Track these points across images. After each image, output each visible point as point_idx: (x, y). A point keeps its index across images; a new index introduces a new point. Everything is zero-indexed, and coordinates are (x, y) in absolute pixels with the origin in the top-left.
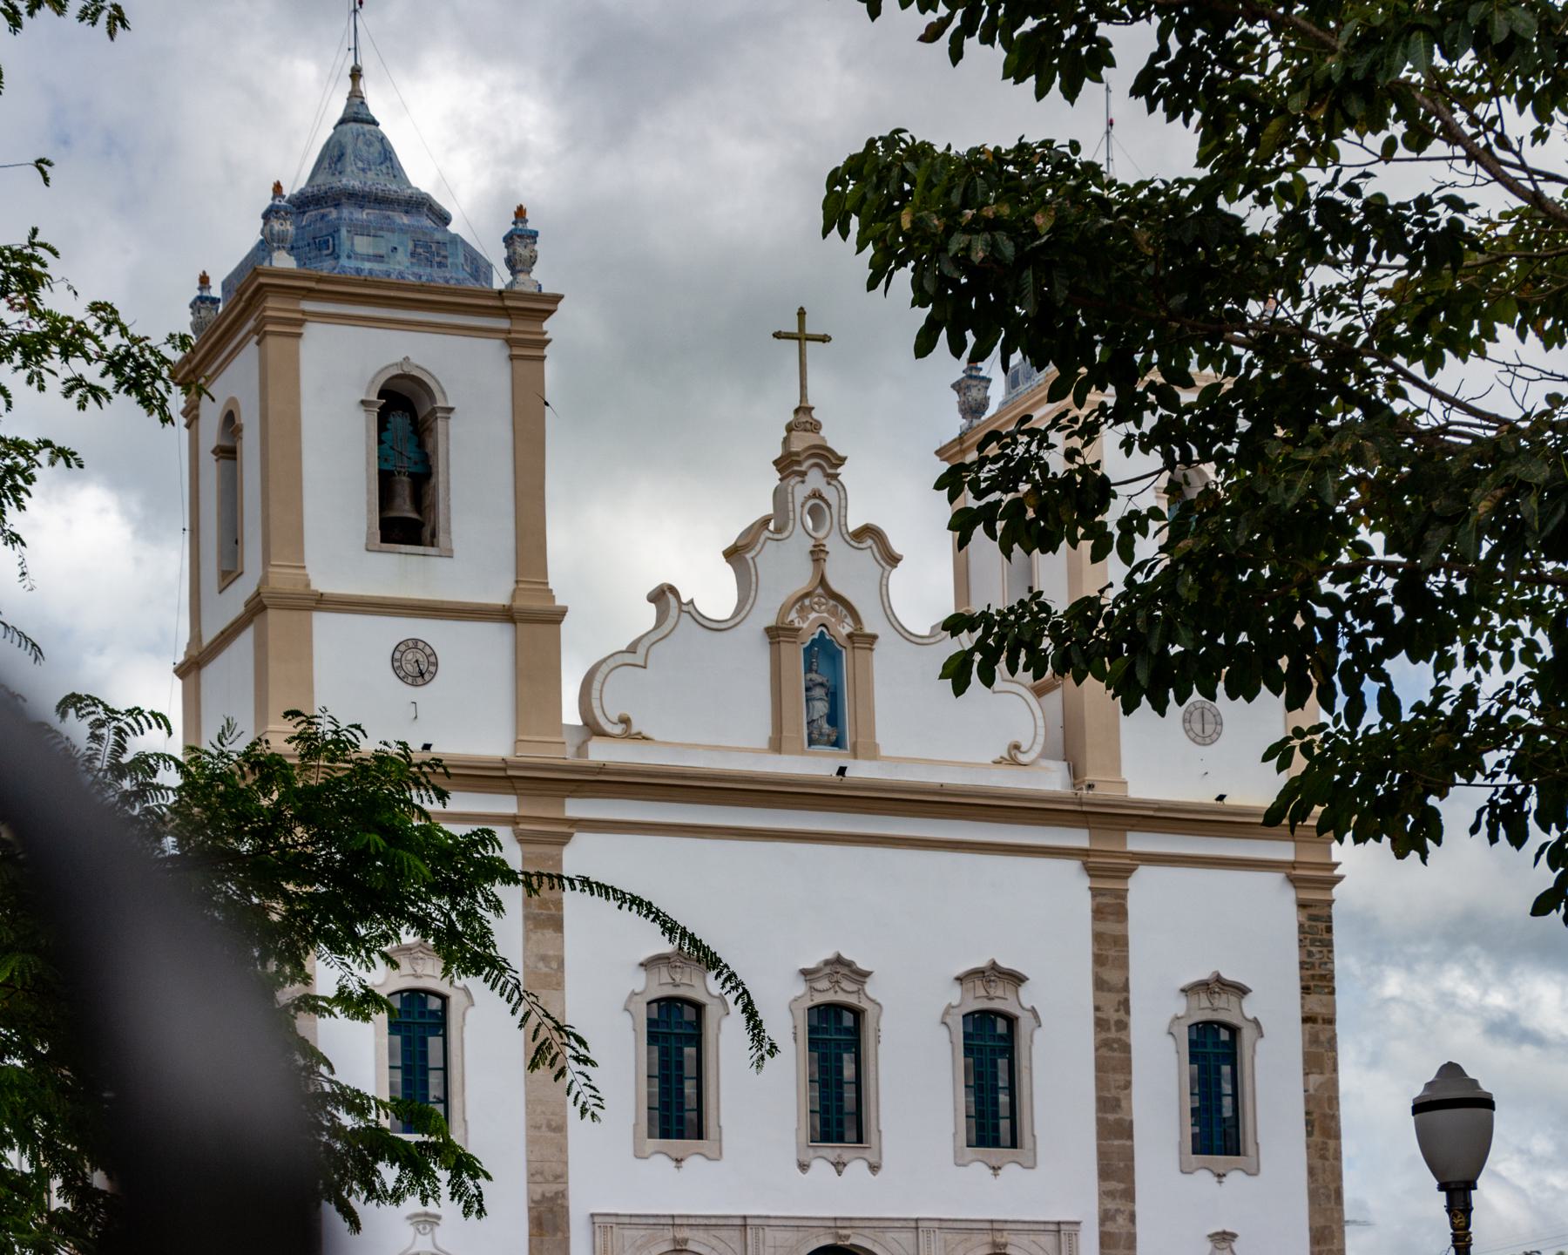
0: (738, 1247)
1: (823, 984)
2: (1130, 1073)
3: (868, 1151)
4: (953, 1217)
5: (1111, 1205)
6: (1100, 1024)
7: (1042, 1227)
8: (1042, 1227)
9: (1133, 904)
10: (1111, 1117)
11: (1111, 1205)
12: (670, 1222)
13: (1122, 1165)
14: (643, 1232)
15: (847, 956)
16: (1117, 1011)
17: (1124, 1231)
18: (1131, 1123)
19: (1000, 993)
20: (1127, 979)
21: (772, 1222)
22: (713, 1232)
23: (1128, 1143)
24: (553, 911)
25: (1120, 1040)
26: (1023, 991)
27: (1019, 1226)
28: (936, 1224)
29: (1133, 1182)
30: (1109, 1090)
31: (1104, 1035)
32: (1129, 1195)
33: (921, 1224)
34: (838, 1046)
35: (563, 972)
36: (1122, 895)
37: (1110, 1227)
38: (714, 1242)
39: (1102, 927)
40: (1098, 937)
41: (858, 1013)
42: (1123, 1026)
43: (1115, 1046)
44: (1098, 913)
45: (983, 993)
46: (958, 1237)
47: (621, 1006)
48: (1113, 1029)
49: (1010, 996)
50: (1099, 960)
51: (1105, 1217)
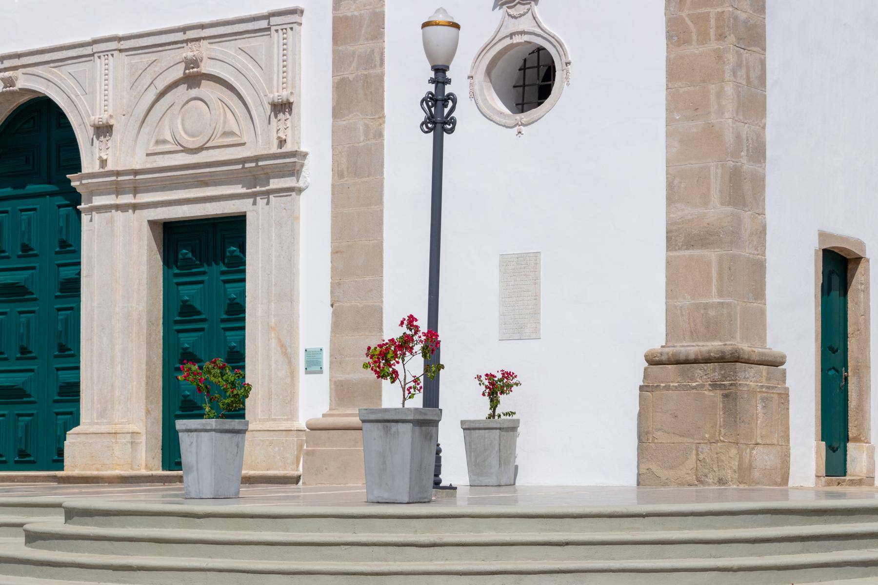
28: (113, 45)
46: (146, 59)
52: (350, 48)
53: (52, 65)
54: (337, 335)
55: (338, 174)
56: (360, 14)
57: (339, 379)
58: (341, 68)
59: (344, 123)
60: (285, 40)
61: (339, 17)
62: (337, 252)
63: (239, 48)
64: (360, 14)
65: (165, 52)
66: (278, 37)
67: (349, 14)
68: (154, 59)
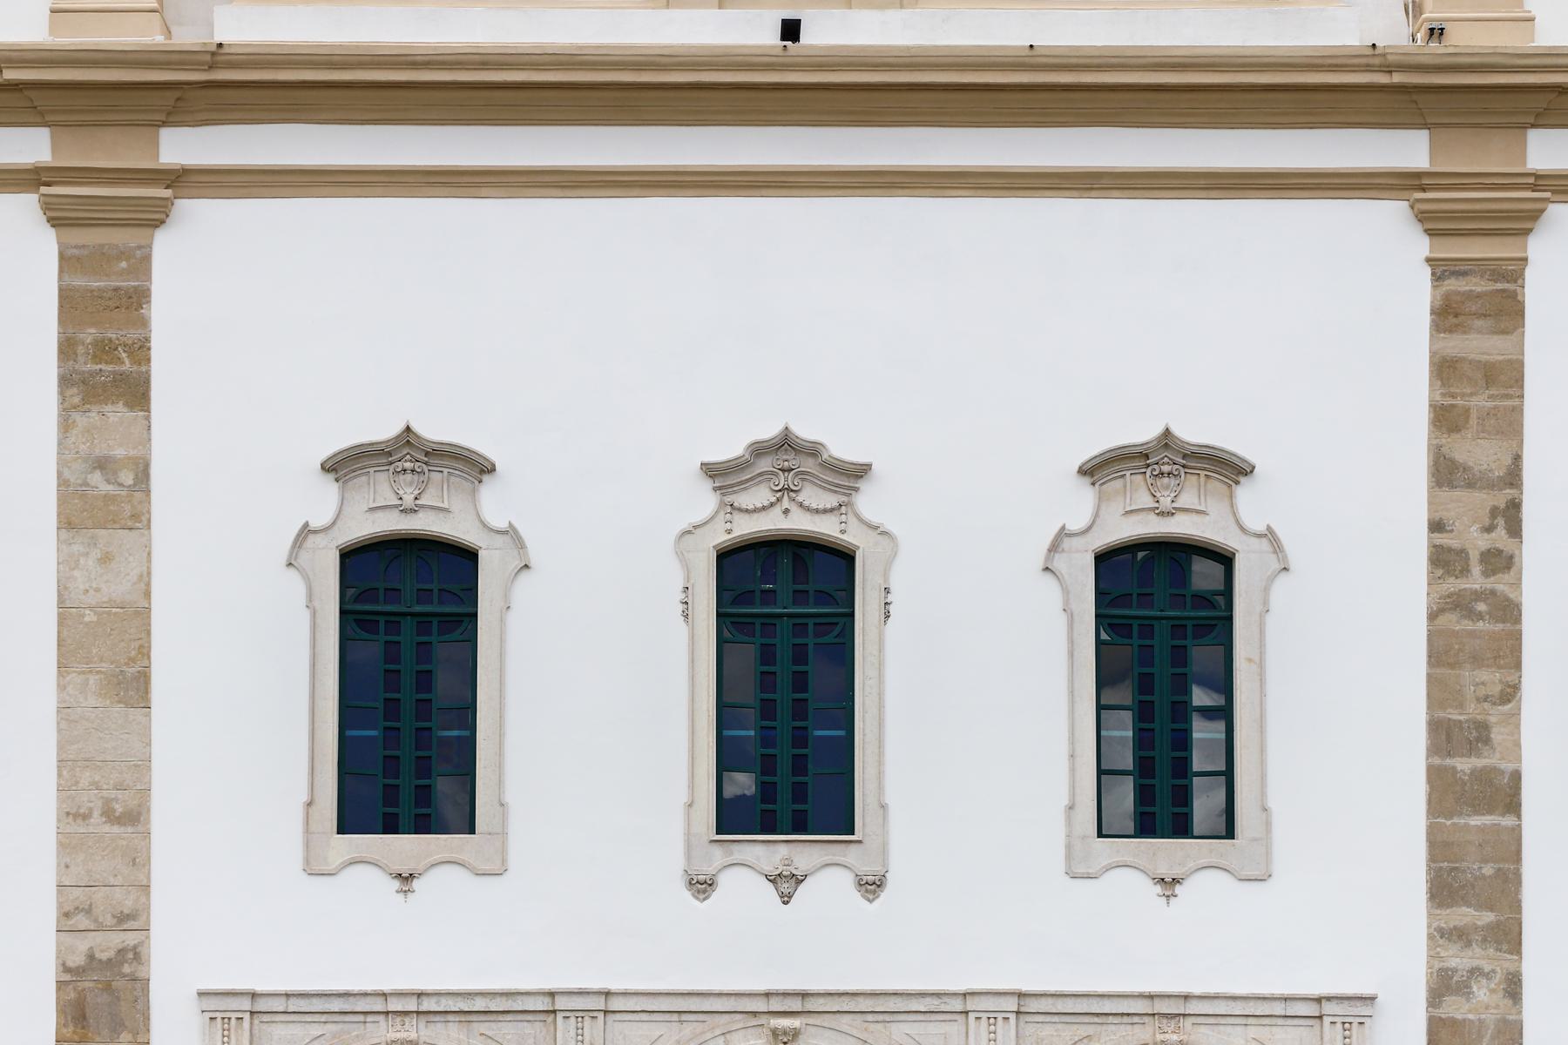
1: (760, 495)
2: (1518, 665)
3: (853, 847)
4: (1052, 988)
5: (1459, 959)
6: (1444, 560)
7: (1278, 1009)
8: (1278, 1009)
9: (1537, 291)
10: (1464, 765)
11: (1459, 959)
12: (379, 1007)
13: (1488, 870)
14: (316, 1030)
15: (805, 432)
16: (1489, 529)
17: (1490, 1017)
18: (1516, 777)
19: (1187, 499)
20: (1518, 458)
22: (483, 1028)
23: (1508, 821)
24: (127, 366)
25: (1493, 593)
26: (1245, 493)
29: (1517, 906)
30: (1461, 706)
31: (1453, 585)
32: (1508, 936)
33: (971, 1004)
34: (800, 628)
35: (148, 492)
36: (1512, 273)
37: (1454, 1008)
39: (1455, 345)
40: (1444, 369)
41: (843, 559)
42: (1501, 562)
43: (1481, 607)
44: (1447, 316)
45: (1145, 500)
47: (284, 561)
48: (1476, 570)
49: (1216, 508)
50: (1445, 419)
51: (1443, 986)
53: (870, 1017)
56: (1479, 1019)
60: (1347, 1040)
61: (1440, 1017)
63: (1254, 1039)
64: (1479, 1019)
65: (1105, 1027)
67: (1459, 1017)
68: (1086, 1035)
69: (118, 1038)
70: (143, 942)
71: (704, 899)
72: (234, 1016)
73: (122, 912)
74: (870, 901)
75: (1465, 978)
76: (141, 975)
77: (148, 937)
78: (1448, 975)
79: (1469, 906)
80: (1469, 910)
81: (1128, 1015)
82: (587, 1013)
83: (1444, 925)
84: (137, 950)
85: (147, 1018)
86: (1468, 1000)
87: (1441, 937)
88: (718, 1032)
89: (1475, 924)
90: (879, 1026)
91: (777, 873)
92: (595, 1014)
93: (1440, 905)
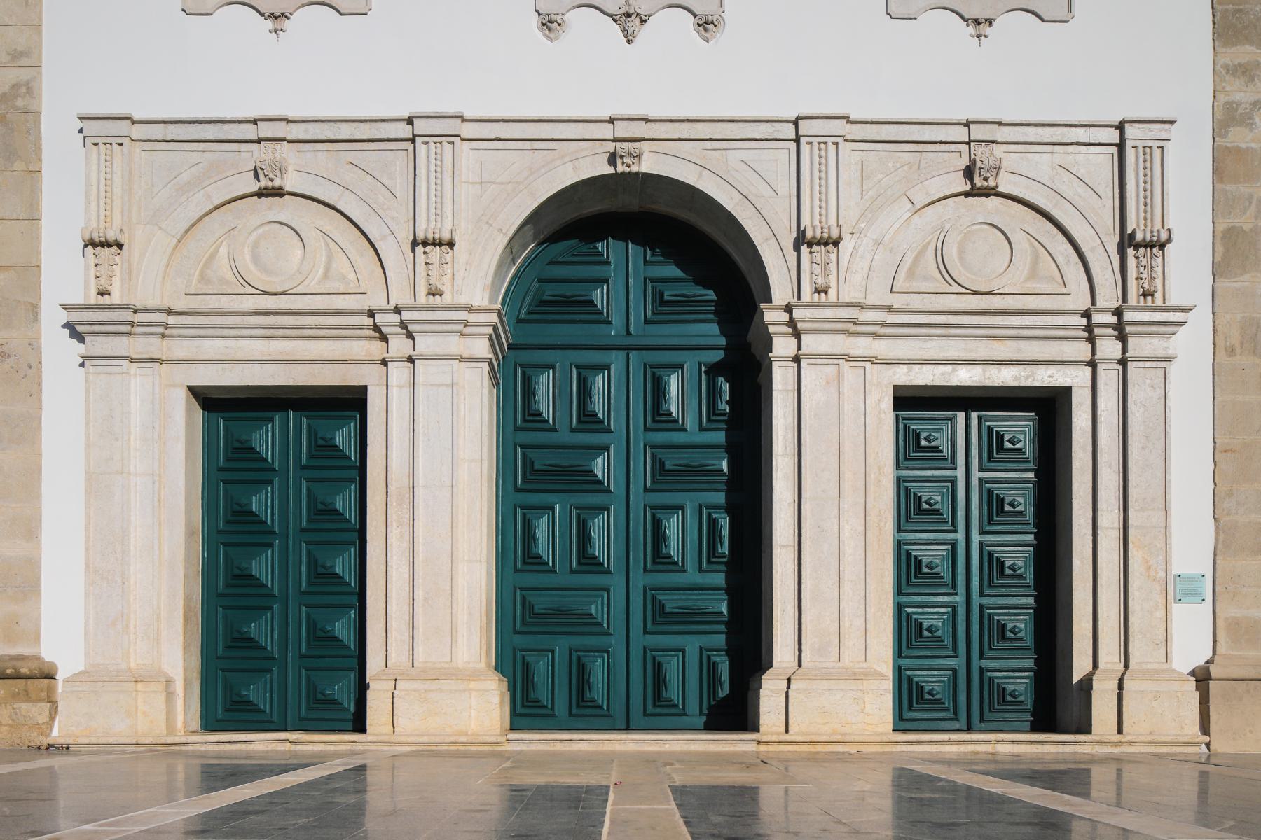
0: (401, 185)
21: (468, 130)
22: (350, 156)
27: (1031, 134)
37: (1238, 137)
38: (350, 176)
52: (1244, 189)
53: (709, 144)
54: (1228, 559)
55: (1226, 348)
57: (1233, 615)
58: (1230, 213)
59: (1237, 285)
61: (1226, 147)
62: (1225, 451)
66: (1137, 156)
67: (1243, 145)
69: (12, 166)
70: (35, 77)
71: (557, 38)
72: (113, 140)
73: (15, 50)
74: (707, 41)
75: (1248, 111)
76: (32, 108)
77: (40, 73)
78: (1233, 108)
79: (1251, 45)
80: (1252, 48)
81: (946, 142)
82: (444, 138)
83: (1230, 63)
84: (30, 85)
85: (38, 149)
86: (1251, 130)
87: (1227, 74)
88: (567, 159)
89: (1258, 61)
90: (716, 153)
91: (622, 11)
92: (452, 139)
93: (1225, 45)
